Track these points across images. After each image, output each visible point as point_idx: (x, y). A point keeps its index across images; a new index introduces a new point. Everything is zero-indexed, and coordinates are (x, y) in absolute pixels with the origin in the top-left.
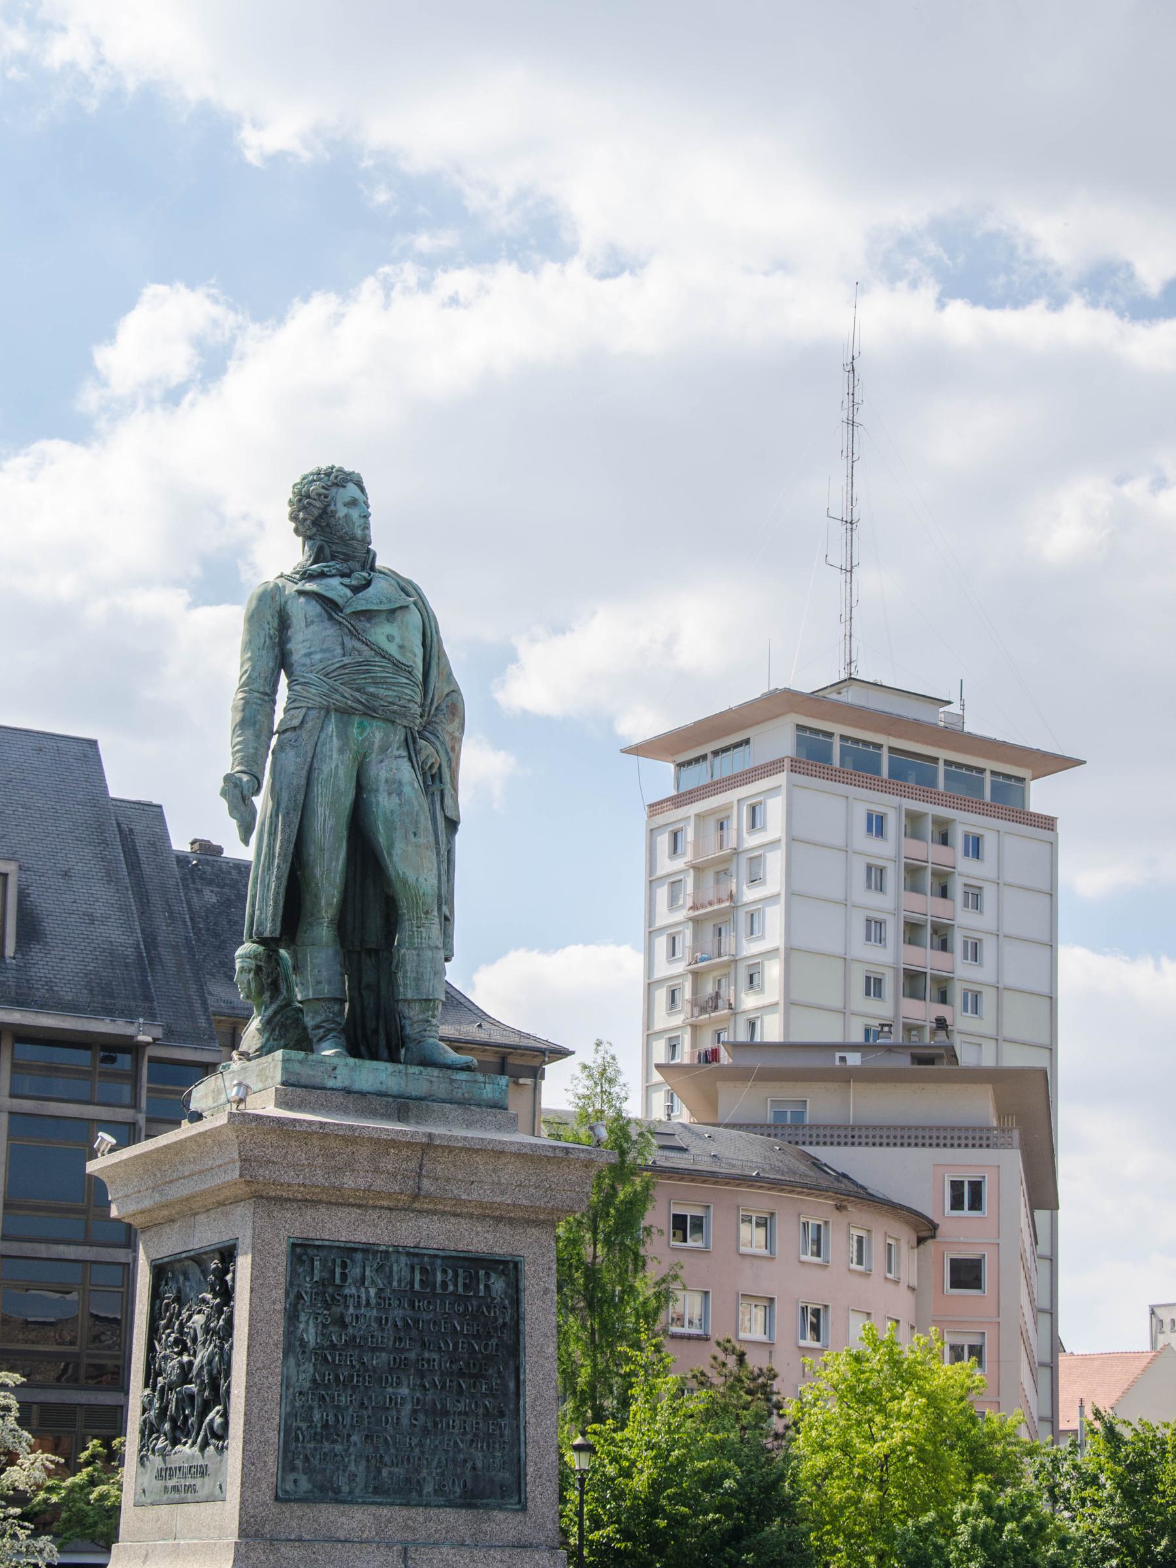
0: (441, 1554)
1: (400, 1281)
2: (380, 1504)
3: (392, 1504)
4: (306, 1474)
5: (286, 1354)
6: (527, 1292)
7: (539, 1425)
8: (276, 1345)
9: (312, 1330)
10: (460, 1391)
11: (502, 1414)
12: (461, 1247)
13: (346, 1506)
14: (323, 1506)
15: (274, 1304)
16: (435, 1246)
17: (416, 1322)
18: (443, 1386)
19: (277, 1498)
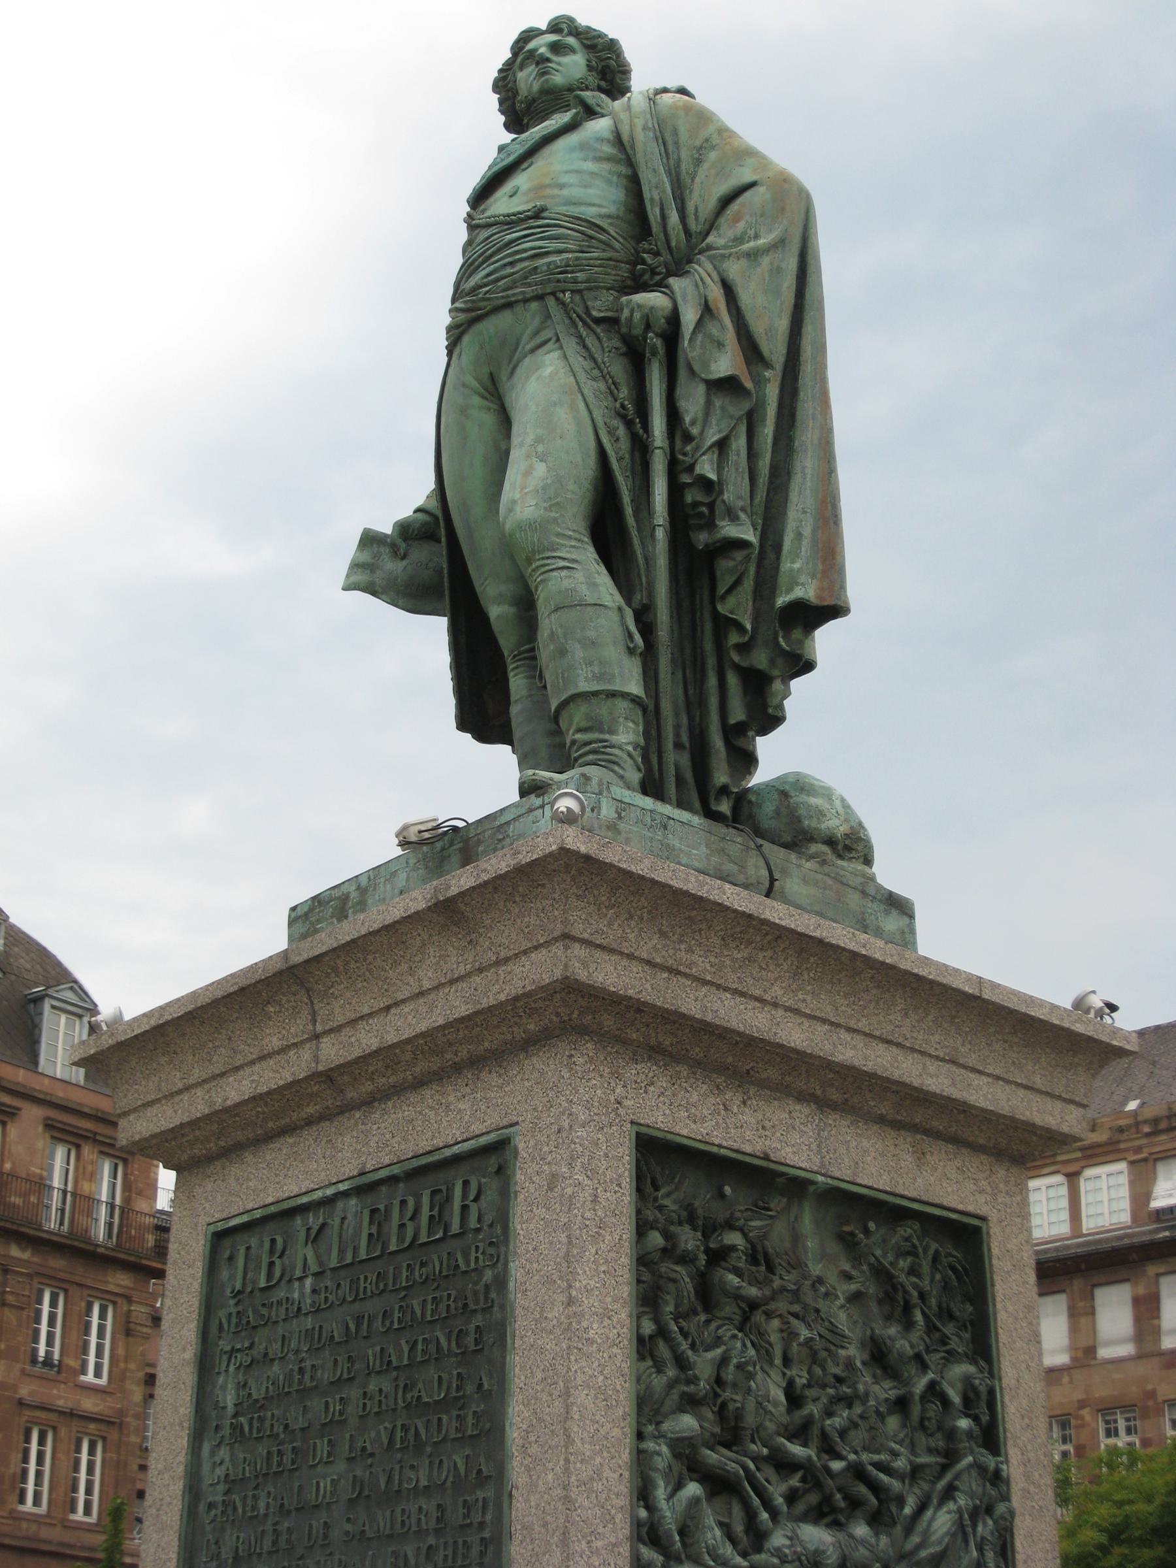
1: (342, 1251)
5: (197, 1438)
6: (521, 1197)
8: (181, 1424)
10: (419, 1446)
11: (482, 1480)
12: (425, 1146)
15: (184, 1349)
16: (387, 1161)
17: (359, 1320)
18: (391, 1441)
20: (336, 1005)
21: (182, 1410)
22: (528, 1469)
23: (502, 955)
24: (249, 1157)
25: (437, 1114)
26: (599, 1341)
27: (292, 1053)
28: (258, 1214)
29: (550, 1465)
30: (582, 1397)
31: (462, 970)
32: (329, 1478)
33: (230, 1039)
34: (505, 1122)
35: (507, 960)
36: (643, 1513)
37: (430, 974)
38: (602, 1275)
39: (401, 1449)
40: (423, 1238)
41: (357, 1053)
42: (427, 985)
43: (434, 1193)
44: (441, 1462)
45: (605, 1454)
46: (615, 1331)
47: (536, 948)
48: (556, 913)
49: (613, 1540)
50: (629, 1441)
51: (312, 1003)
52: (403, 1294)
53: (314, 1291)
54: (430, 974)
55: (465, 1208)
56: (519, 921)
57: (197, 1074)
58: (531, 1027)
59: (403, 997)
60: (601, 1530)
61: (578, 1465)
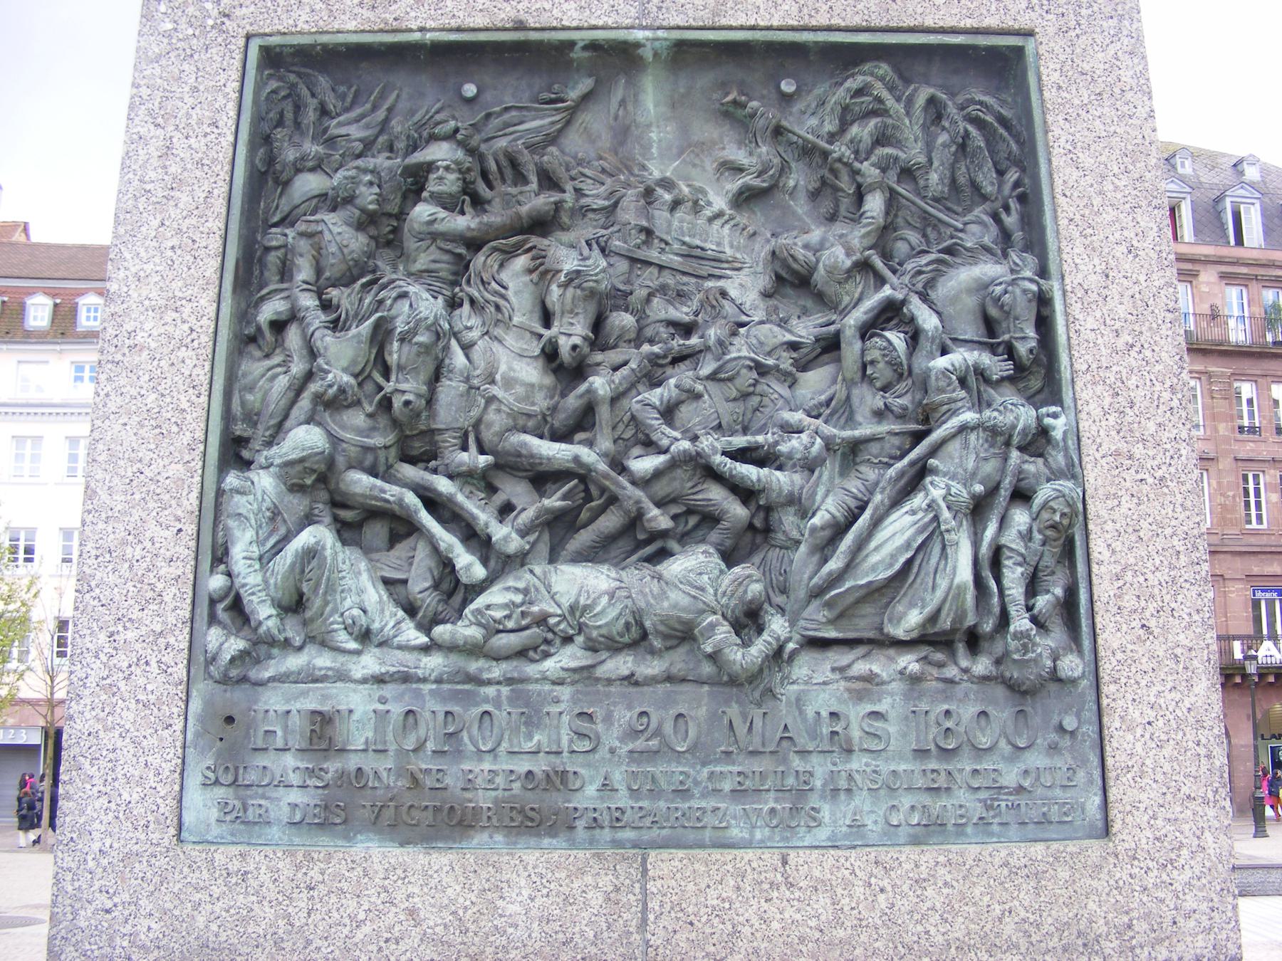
26: (153, 345)
38: (169, 253)
45: (151, 505)
49: (158, 628)
60: (135, 614)
61: (101, 526)
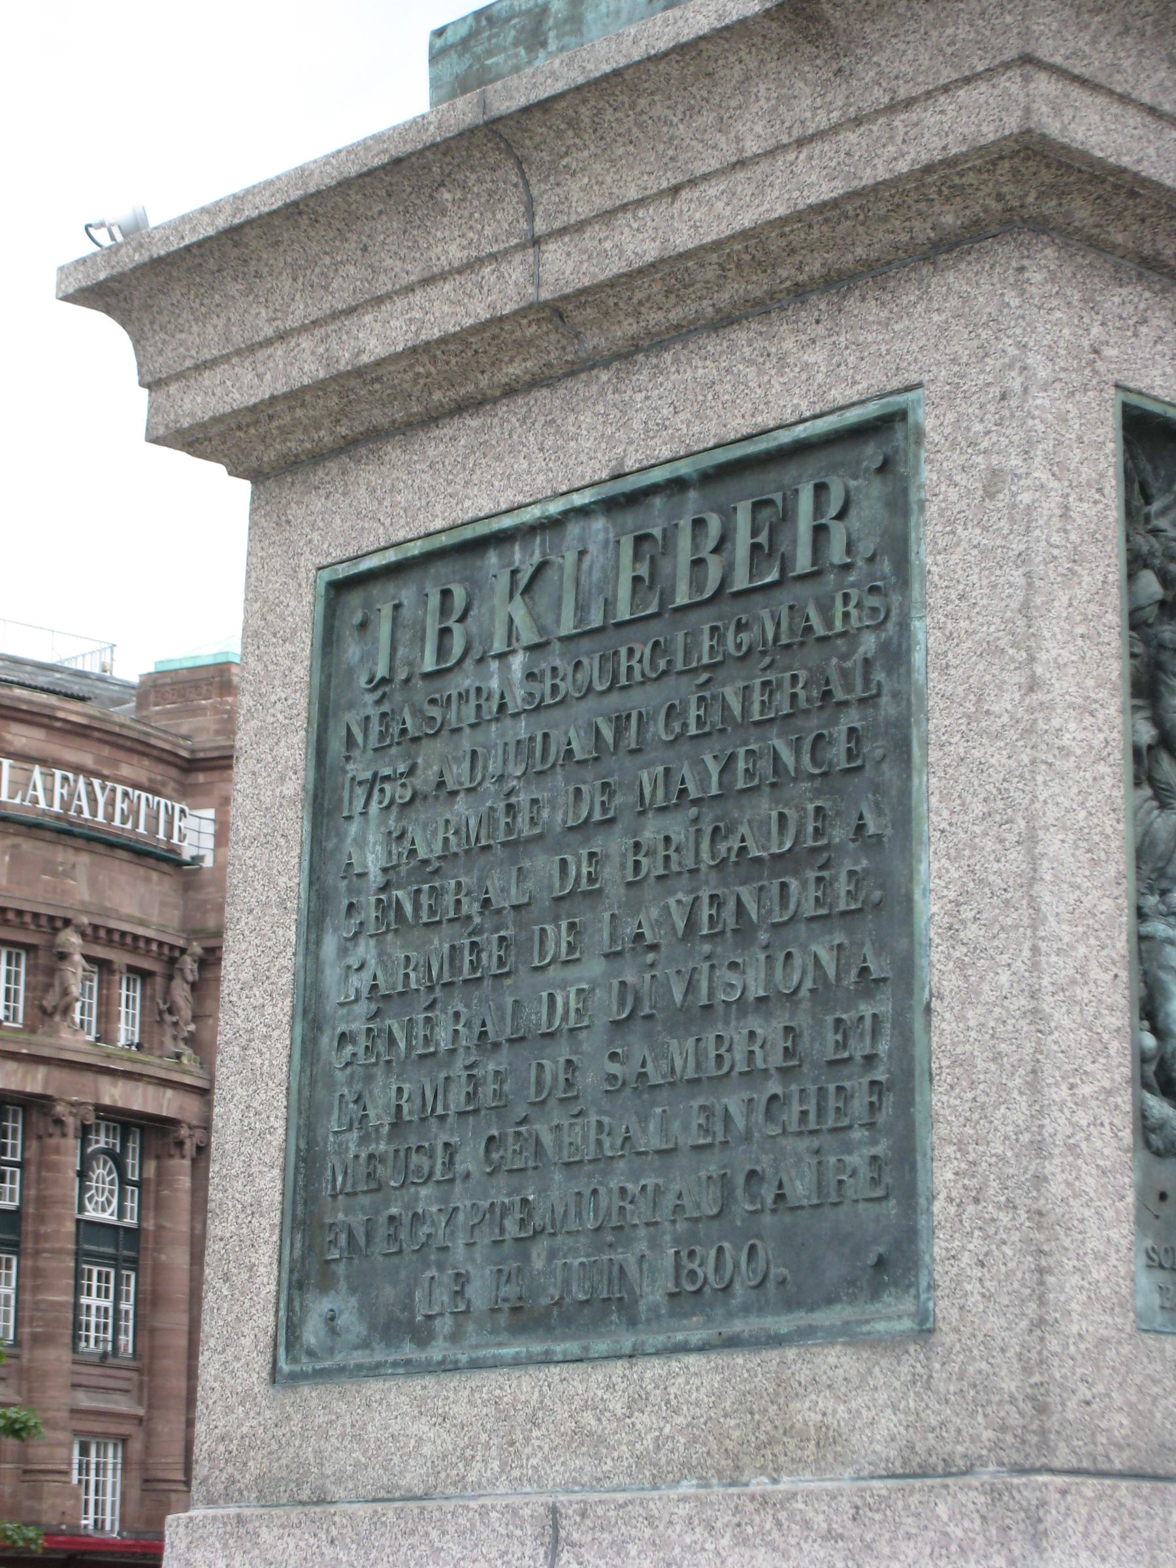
0: (650, 1520)
1: (581, 609)
2: (515, 1363)
3: (546, 1360)
4: (352, 1290)
6: (932, 509)
7: (971, 995)
8: (282, 903)
9: (374, 837)
10: (744, 931)
11: (868, 984)
12: (739, 425)
13: (430, 1381)
14: (374, 1388)
15: (282, 779)
16: (666, 453)
17: (620, 722)
18: (691, 924)
19: (274, 1375)
20: (574, 187)
21: (282, 881)
22: (961, 966)
23: (902, 93)
24: (393, 452)
25: (760, 373)
26: (1078, 752)
27: (487, 270)
28: (415, 549)
29: (1005, 959)
30: (1053, 844)
31: (822, 120)
32: (577, 986)
33: (365, 249)
34: (895, 384)
35: (909, 103)
36: (1150, 1041)
37: (758, 129)
38: (1080, 642)
39: (710, 937)
40: (741, 582)
41: (616, 267)
42: (752, 147)
43: (757, 506)
44: (789, 956)
46: (1101, 736)
47: (967, 80)
48: (1009, 19)
49: (1107, 1084)
50: (1126, 918)
51: (527, 184)
52: (704, 677)
53: (530, 676)
54: (758, 129)
55: (820, 531)
56: (934, 34)
57: (300, 311)
58: (948, 219)
59: (705, 169)
60: (1089, 1068)
61: (1054, 958)
